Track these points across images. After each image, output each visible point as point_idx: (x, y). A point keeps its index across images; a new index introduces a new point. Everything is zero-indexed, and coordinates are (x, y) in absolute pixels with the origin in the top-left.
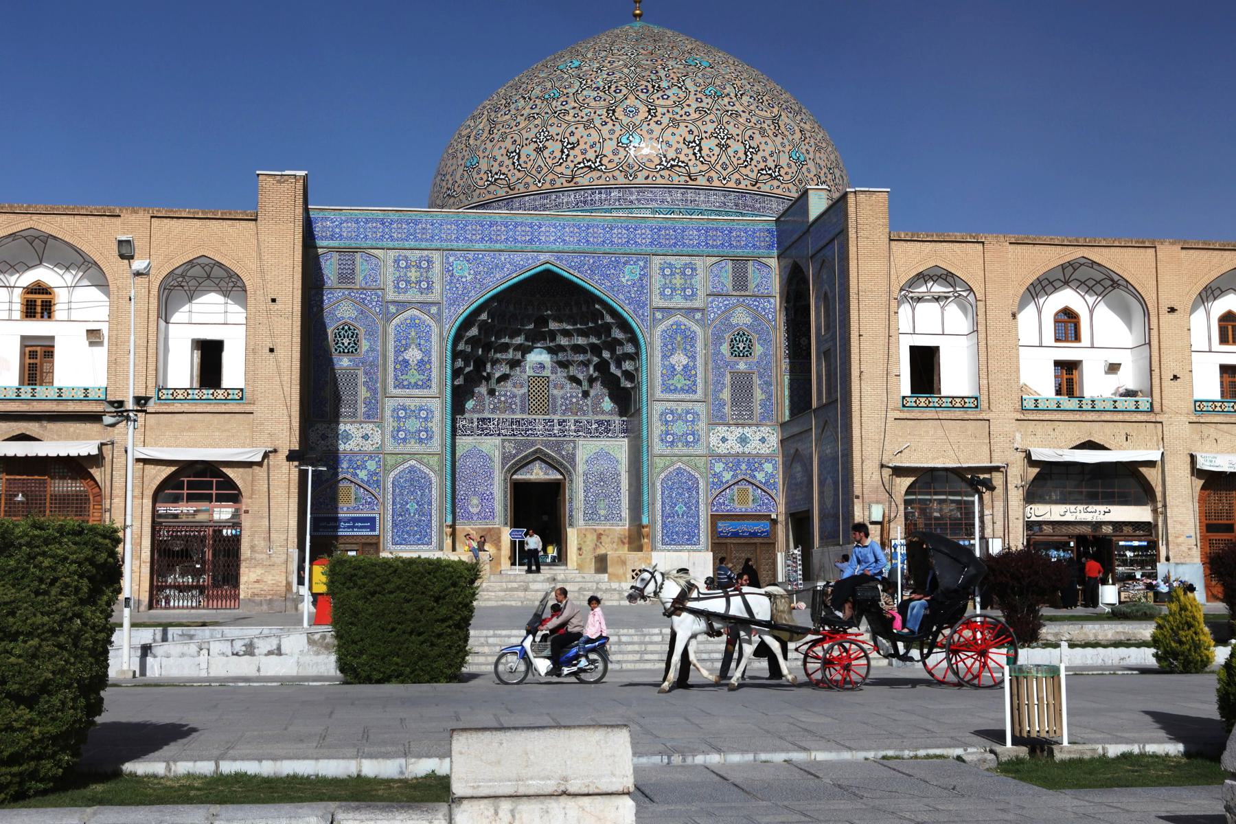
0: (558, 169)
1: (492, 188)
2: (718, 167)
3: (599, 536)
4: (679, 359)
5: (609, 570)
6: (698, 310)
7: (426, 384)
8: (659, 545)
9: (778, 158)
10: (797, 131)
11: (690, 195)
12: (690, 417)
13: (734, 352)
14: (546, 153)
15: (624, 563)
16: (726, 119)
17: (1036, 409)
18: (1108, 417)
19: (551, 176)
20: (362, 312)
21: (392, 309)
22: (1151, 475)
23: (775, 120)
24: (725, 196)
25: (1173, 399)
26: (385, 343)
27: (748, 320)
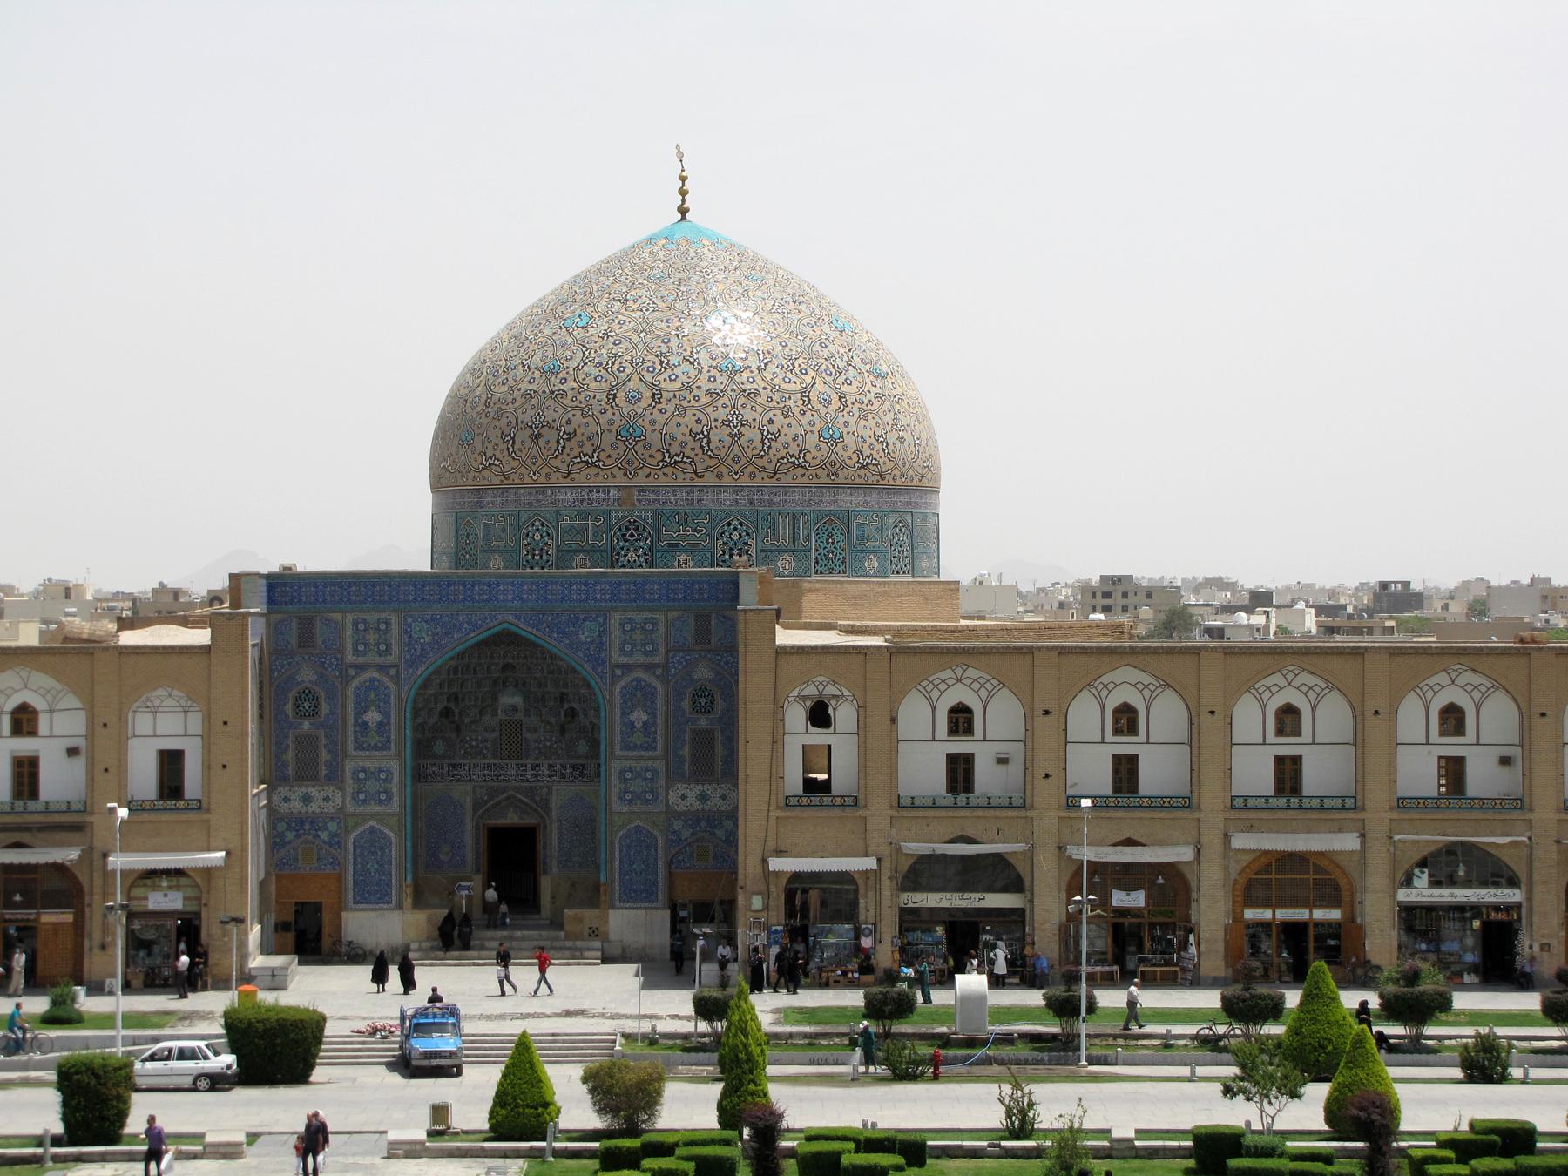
0: (554, 463)
1: (486, 473)
2: (729, 461)
3: (573, 884)
4: (639, 716)
5: (567, 927)
6: (658, 666)
7: (385, 746)
8: (617, 904)
9: (804, 441)
10: (835, 397)
11: (696, 495)
12: (649, 775)
13: (695, 707)
14: (542, 442)
15: (581, 920)
16: (742, 400)
17: (913, 806)
18: (980, 813)
19: (546, 470)
20: (322, 676)
21: (352, 672)
22: (1021, 867)
23: (805, 395)
24: (736, 492)
25: (1046, 796)
26: (344, 706)
27: (711, 675)
